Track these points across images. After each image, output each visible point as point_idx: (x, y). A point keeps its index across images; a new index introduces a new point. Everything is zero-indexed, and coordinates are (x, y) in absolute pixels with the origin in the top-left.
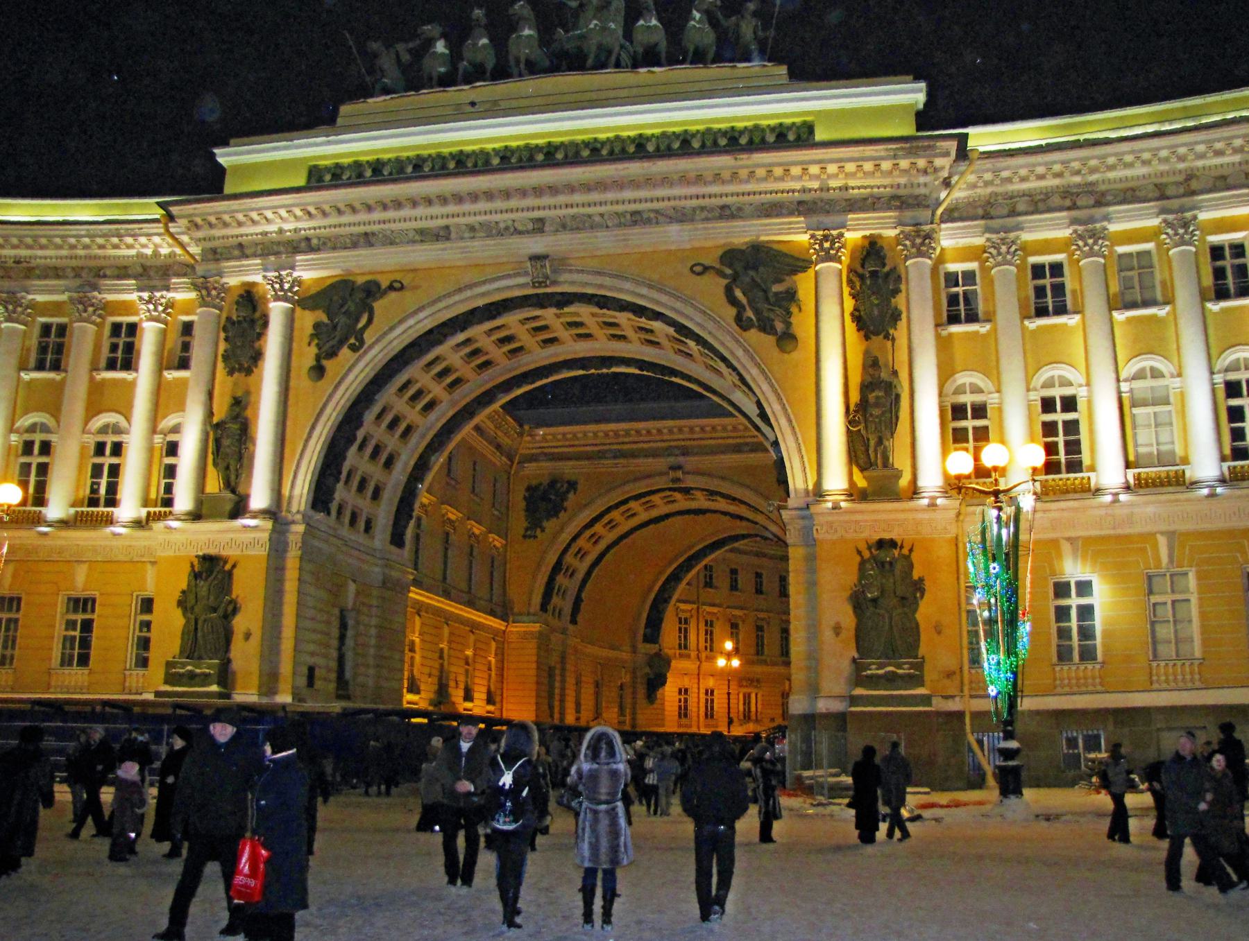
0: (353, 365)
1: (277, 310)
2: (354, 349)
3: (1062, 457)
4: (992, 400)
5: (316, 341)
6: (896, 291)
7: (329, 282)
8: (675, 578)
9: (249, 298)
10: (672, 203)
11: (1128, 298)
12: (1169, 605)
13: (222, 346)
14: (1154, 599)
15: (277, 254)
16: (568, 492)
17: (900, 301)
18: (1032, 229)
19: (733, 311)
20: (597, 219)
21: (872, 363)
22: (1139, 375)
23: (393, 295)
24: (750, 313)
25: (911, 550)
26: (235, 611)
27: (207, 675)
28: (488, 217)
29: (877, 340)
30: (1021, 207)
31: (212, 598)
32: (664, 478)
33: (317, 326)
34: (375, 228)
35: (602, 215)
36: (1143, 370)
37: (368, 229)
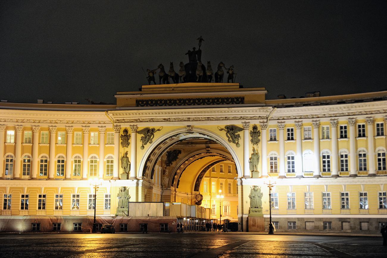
0: (151, 146)
4: (278, 157)
5: (142, 141)
6: (259, 136)
10: (216, 116)
12: (309, 199)
13: (121, 141)
14: (306, 197)
16: (179, 153)
17: (260, 138)
19: (228, 138)
21: (254, 150)
24: (231, 139)
25: (260, 188)
26: (130, 198)
28: (178, 117)
29: (255, 146)
31: (125, 195)
33: (142, 137)
34: (154, 118)
35: (202, 118)
37: (152, 118)
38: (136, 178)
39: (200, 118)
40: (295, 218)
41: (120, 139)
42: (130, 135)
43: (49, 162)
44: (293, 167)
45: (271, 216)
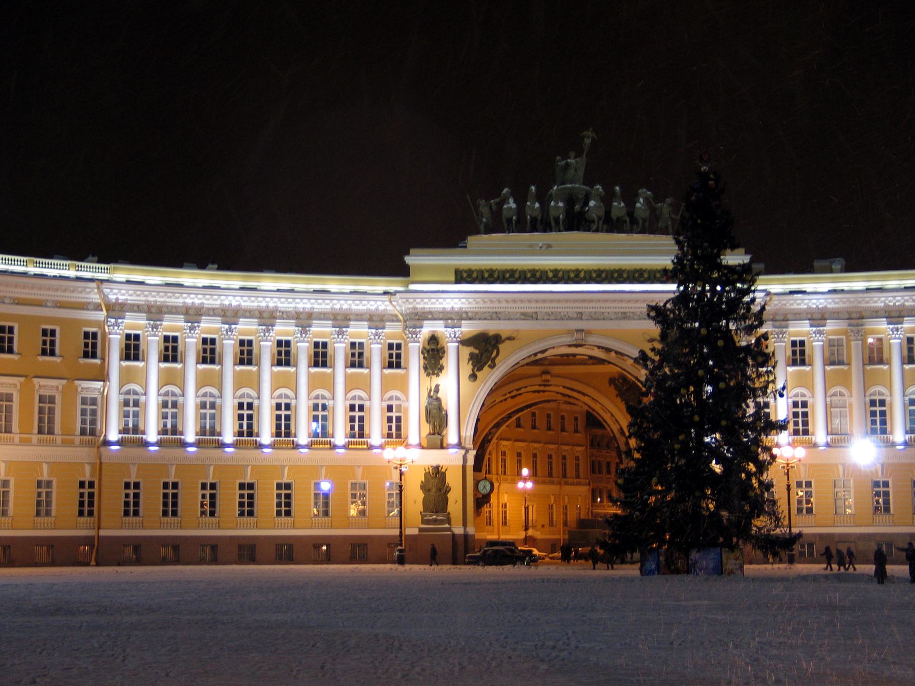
1: (451, 348)
2: (492, 366)
3: (801, 427)
7: (474, 333)
8: (498, 425)
9: (433, 339)
11: (832, 359)
15: (451, 319)
18: (793, 327)
20: (606, 314)
22: (834, 395)
23: (508, 342)
27: (442, 520)
30: (789, 317)
32: (539, 378)
36: (836, 392)
37: (497, 310)
38: (459, 445)
39: (606, 314)
40: (814, 535)
41: (422, 356)
42: (443, 348)
43: (259, 407)
44: (805, 423)
45: (790, 531)
